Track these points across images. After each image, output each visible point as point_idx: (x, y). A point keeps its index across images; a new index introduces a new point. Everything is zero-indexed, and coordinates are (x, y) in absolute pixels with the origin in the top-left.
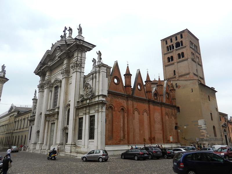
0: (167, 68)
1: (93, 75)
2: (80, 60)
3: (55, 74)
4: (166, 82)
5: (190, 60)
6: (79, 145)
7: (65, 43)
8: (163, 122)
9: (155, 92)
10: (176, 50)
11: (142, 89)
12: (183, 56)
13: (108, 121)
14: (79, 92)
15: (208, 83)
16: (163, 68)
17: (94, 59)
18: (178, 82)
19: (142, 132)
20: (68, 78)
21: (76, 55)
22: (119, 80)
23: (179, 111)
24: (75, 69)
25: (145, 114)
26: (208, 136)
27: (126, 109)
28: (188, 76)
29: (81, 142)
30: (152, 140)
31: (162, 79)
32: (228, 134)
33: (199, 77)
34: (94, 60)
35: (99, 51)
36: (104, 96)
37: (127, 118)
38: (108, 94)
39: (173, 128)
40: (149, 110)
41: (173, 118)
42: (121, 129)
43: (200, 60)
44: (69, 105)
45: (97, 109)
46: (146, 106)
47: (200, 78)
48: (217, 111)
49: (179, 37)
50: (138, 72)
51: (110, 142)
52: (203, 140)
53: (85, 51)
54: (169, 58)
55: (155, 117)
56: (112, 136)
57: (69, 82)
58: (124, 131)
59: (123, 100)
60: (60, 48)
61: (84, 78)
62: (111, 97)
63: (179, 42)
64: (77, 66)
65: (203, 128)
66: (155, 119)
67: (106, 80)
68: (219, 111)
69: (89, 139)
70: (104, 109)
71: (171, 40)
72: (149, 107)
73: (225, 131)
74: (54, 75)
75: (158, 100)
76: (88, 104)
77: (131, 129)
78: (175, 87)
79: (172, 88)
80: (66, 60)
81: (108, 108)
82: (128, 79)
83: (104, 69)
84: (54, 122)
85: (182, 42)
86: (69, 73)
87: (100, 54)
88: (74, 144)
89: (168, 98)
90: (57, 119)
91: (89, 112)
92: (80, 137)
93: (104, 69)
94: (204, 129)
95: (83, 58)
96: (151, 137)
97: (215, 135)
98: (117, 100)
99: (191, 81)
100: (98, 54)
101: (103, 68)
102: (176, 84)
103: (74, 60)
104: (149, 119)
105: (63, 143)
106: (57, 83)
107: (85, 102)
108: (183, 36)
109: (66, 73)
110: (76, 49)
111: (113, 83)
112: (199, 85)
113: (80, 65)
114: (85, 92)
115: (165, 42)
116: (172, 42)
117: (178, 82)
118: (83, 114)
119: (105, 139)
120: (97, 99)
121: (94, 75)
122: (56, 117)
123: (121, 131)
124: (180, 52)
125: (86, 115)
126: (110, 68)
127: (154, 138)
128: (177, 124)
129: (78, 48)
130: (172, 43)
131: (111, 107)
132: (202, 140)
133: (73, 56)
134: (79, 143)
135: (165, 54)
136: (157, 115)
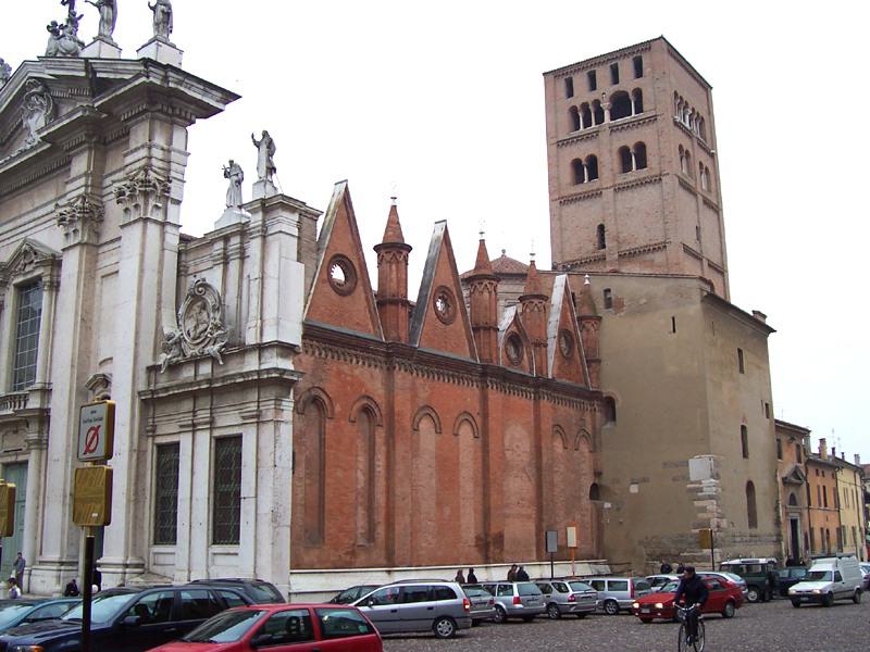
0: (571, 209)
1: (230, 242)
2: (160, 164)
3: (20, 217)
4: (561, 279)
5: (669, 183)
6: (158, 569)
7: (83, 74)
8: (539, 469)
9: (514, 329)
10: (613, 129)
11: (455, 315)
13: (303, 465)
14: (158, 321)
15: (742, 296)
16: (551, 210)
17: (231, 162)
18: (615, 284)
19: (447, 511)
20: (93, 247)
21: (139, 135)
22: (355, 269)
23: (614, 419)
24: (136, 206)
25: (465, 431)
26: (724, 523)
27: (383, 407)
28: (658, 257)
29: (171, 557)
30: (492, 548)
31: (544, 263)
32: (805, 512)
33: (705, 263)
34: (233, 172)
35: (265, 134)
36: (286, 349)
37: (384, 448)
38: (304, 337)
39: (582, 494)
40: (485, 415)
41: (587, 450)
42: (360, 500)
43: (713, 185)
44: (105, 381)
45: (253, 406)
46: (467, 395)
47: (711, 265)
48: (768, 417)
49: (626, 67)
50: (440, 233)
51: (313, 555)
53: (185, 119)
54: (577, 164)
55: (507, 443)
56: (321, 530)
57: (100, 265)
58: (370, 509)
59: (370, 366)
60: (47, 88)
61: (180, 253)
62: (317, 353)
63: (625, 94)
64: (146, 195)
65: (708, 491)
66: (508, 453)
67: (296, 275)
68: (776, 417)
69: (214, 543)
70: (288, 405)
71: (592, 78)
72: (484, 399)
73: (793, 500)
75: (522, 368)
76: (209, 381)
77: (404, 499)
78: (600, 304)
79: (586, 311)
80: (86, 154)
81: (305, 403)
82: (394, 267)
83: (287, 222)
84: (21, 458)
85: (638, 93)
86: (101, 220)
87: (266, 144)
88: (141, 562)
89: (565, 357)
90: (42, 444)
91: (212, 422)
92: (165, 531)
93: (287, 222)
94: (711, 497)
95: (174, 156)
96: (487, 535)
97: (753, 522)
98: (345, 368)
99: (671, 282)
100: (257, 144)
101: (285, 215)
102: (607, 291)
103: (134, 159)
104: (480, 454)
105: (77, 556)
106: (27, 269)
107: (187, 373)
108: (646, 70)
109: (84, 221)
110: (145, 111)
111: (327, 288)
112: (702, 301)
113: (157, 189)
114: (190, 325)
115: (562, 85)
116: (593, 87)
117: (615, 284)
118: (181, 426)
119: (292, 544)
120: (251, 364)
121: (235, 241)
122: (33, 436)
123: (360, 508)
124: (629, 139)
125: (194, 432)
126: (313, 216)
127: (500, 538)
128: (598, 474)
129: (152, 103)
130: (595, 95)
131: (316, 401)
133: (124, 136)
134: (161, 559)
135: (561, 144)
136: (516, 440)
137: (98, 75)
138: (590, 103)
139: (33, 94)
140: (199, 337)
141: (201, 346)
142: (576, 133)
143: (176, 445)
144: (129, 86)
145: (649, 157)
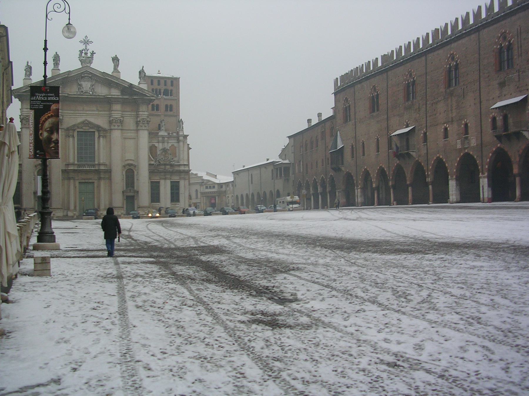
3: (78, 110)
49: (169, 82)
84: (90, 181)
85: (171, 90)
106: (84, 128)
116: (159, 84)
124: (169, 103)
134: (154, 206)
143: (159, 182)
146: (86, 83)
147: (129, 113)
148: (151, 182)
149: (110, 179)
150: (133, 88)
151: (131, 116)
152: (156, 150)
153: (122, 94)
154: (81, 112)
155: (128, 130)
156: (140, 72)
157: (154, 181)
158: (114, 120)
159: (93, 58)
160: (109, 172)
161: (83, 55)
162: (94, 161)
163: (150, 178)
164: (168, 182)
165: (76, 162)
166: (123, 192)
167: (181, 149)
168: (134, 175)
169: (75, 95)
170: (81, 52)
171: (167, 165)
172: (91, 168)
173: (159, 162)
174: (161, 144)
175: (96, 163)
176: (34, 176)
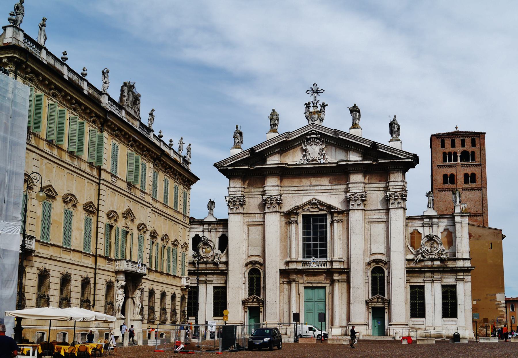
3: (304, 186)
7: (370, 146)
10: (463, 165)
12: (474, 181)
28: (480, 219)
49: (468, 141)
52: (501, 322)
54: (445, 176)
63: (468, 152)
74: (296, 189)
85: (473, 153)
106: (311, 210)
115: (439, 142)
116: (453, 145)
118: (425, 281)
120: (460, 264)
124: (469, 171)
132: (500, 322)
134: (415, 323)
137: (379, 150)
138: (453, 153)
139: (314, 138)
140: (432, 252)
141: (433, 255)
142: (444, 163)
143: (423, 287)
144: (401, 161)
145: (477, 180)
146: (314, 147)
147: (377, 185)
148: (411, 287)
149: (348, 281)
150: (378, 148)
151: (378, 189)
152: (420, 237)
153: (365, 158)
154: (308, 188)
155: (375, 210)
156: (391, 125)
157: (415, 284)
158: (353, 197)
159: (324, 111)
160: (346, 272)
161: (311, 109)
162: (326, 257)
163: (408, 281)
164: (438, 288)
165: (301, 259)
166: (367, 303)
167: (458, 234)
168: (384, 277)
169: (297, 164)
170: (308, 106)
171: (436, 260)
172: (320, 267)
173: (423, 257)
174: (427, 229)
175: (329, 259)
176: (244, 279)
